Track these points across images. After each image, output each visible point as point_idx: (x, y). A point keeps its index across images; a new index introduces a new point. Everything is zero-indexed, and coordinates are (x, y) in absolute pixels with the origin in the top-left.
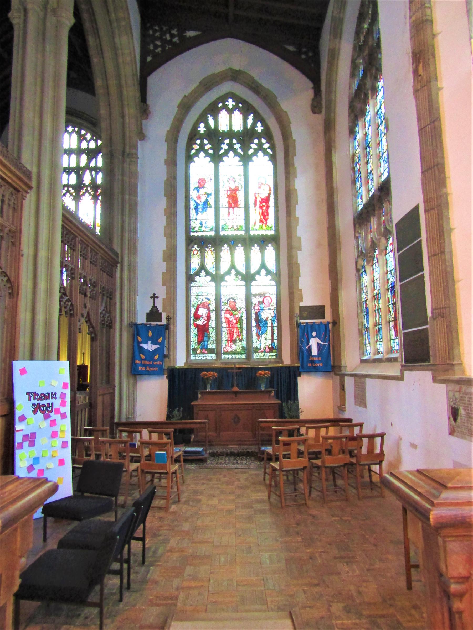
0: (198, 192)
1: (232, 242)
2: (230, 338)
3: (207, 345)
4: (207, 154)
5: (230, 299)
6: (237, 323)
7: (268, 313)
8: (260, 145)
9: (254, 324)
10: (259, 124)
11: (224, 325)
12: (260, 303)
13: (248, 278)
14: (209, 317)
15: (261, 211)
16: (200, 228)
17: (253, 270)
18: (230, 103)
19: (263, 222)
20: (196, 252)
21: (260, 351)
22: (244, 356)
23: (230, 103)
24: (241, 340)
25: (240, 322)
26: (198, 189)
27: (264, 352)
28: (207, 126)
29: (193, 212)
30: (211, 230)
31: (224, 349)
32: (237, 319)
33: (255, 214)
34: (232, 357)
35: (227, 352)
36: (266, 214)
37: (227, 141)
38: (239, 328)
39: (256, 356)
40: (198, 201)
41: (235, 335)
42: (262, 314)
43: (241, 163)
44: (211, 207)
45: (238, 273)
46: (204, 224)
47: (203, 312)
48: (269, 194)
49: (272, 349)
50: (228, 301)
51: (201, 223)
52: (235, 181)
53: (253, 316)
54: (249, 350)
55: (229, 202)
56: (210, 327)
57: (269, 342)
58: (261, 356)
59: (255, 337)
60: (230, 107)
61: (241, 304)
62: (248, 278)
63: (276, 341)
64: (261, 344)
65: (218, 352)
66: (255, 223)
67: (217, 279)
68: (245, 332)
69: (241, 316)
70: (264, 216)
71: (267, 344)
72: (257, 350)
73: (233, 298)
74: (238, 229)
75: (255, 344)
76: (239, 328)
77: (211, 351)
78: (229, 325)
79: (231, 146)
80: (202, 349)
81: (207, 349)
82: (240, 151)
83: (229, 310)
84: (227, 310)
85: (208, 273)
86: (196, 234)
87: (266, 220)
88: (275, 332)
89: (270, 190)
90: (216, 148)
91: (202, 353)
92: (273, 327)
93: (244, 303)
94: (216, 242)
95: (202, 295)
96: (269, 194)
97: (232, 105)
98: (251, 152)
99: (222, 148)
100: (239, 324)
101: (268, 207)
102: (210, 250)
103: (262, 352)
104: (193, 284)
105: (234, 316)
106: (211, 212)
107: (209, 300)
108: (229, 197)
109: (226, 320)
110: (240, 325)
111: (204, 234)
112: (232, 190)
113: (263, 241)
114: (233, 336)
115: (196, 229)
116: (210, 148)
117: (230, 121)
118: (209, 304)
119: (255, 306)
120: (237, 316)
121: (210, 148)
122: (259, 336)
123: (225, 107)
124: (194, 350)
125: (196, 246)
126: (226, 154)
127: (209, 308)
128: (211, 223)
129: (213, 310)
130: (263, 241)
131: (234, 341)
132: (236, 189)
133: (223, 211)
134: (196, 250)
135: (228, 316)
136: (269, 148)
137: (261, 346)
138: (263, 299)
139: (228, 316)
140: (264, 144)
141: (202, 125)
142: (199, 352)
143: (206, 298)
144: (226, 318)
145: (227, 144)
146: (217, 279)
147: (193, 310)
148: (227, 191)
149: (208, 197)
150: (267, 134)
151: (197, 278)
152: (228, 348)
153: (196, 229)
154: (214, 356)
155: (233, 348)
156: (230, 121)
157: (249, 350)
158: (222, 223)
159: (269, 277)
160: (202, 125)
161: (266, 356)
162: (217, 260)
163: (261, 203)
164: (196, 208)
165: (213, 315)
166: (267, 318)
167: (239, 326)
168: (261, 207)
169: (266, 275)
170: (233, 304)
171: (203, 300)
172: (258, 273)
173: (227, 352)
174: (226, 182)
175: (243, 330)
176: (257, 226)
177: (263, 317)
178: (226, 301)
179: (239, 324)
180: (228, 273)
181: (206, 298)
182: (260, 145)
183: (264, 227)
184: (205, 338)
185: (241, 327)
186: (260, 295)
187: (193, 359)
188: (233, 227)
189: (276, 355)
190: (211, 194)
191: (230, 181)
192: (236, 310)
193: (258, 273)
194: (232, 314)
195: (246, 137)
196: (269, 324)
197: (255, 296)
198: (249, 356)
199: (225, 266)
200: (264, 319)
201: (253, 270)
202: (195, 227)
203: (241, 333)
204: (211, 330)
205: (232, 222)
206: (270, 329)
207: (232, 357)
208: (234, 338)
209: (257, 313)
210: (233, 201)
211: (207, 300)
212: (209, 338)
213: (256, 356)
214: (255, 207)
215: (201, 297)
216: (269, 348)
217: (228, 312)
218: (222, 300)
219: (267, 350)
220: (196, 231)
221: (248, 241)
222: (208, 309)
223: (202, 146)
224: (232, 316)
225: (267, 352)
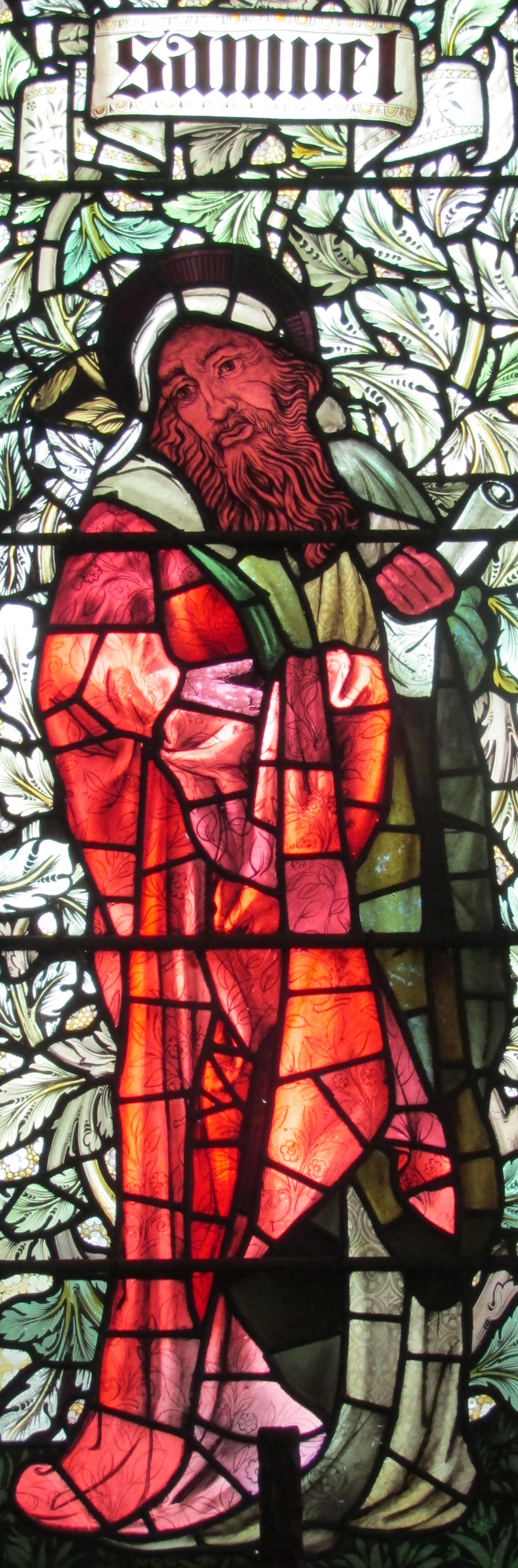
2: (183, 1205)
5: (164, 272)
6: (347, 852)
25: (431, 826)
38: (401, 973)
50: (124, 310)
76: (401, 973)
83: (160, 539)
100: (388, 859)
105: (284, 661)
109: (90, 781)
110: (431, 877)
114: (254, 1159)
120: (349, 679)
131: (291, 1298)
135: (133, 671)
139: (133, 671)
170: (252, 391)
178: (70, 325)
179: (388, 859)
192: (332, 525)
194: (235, 632)
208: (286, 1205)
217: (116, 583)
224: (216, 686)
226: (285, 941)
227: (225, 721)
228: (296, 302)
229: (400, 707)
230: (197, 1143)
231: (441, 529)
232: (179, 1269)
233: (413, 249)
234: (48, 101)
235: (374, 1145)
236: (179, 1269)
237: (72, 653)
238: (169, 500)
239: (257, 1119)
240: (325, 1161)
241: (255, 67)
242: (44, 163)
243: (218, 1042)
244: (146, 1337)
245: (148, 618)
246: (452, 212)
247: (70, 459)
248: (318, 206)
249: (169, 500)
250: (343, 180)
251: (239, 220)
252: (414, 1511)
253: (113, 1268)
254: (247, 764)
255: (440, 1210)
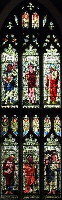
0: (7, 75)
1: (31, 113)
3: (12, 188)
4: (14, 46)
5: (29, 155)
6: (33, 173)
7: (55, 166)
8: (52, 40)
9: (45, 174)
10: (51, 24)
11: (24, 174)
12: (50, 158)
13: (41, 140)
14: (14, 168)
15: (51, 90)
16: (8, 102)
17: (45, 135)
18: (31, 6)
19: (53, 99)
20: (5, 120)
21: (49, 193)
22: (38, 197)
23: (31, 6)
24: (36, 185)
26: (7, 73)
27: (52, 194)
28: (14, 23)
29: (3, 90)
30: (16, 104)
31: (24, 191)
32: (33, 170)
33: (47, 94)
34: (30, 197)
35: (26, 194)
36: (55, 93)
37: (28, 36)
39: (45, 197)
40: (7, 82)
41: (32, 182)
42: (51, 166)
43: (37, 54)
44: (16, 86)
45: (34, 136)
46: (11, 98)
47: (10, 164)
48: (58, 78)
49: (57, 192)
51: (9, 98)
52: (33, 67)
53: (45, 167)
54: (41, 192)
55: (28, 83)
56: (15, 175)
57: (56, 187)
58: (50, 197)
59: (45, 183)
60: (31, 9)
61: (36, 159)
62: (41, 140)
63: (60, 186)
64: (49, 188)
65: (20, 193)
66: (47, 99)
67: (20, 140)
68: (38, 179)
69: (37, 168)
70: (54, 94)
71: (54, 188)
72: (47, 192)
73: (30, 155)
74: (34, 104)
75: (46, 188)
76: (35, 177)
77: (15, 193)
78: (28, 174)
79: (31, 39)
80: (9, 192)
81: (13, 192)
82: (37, 44)
84: (26, 163)
85: (14, 136)
86: (5, 107)
87: (55, 97)
88: (60, 180)
89: (58, 74)
90: (20, 41)
91: (9, 194)
92: (58, 176)
93: (39, 159)
94: (20, 113)
95: (9, 152)
96: (58, 78)
97: (32, 8)
98: (45, 44)
99: (24, 42)
100: (34, 173)
101: (57, 87)
102: (15, 119)
103: (50, 194)
104: (3, 144)
105: (31, 167)
106: (16, 90)
107: (14, 155)
108: (29, 79)
111: (11, 107)
112: (30, 74)
113: (52, 113)
115: (5, 103)
116: (16, 42)
117: (31, 21)
118: (14, 159)
119: (46, 161)
121: (16, 42)
122: (48, 182)
123: (27, 9)
124: (4, 192)
125: (5, 116)
126: (27, 46)
127: (14, 162)
128: (16, 99)
129: (17, 163)
130: (52, 113)
131: (31, 186)
132: (34, 73)
133: (25, 89)
134: (5, 118)
135: (27, 167)
136: (58, 42)
137: (49, 190)
138: (52, 156)
139: (27, 167)
140: (54, 39)
141: (10, 23)
142: (7, 193)
143: (12, 154)
144: (26, 169)
145: (28, 39)
146: (20, 140)
147: (3, 162)
148: (28, 74)
149: (14, 79)
150: (56, 31)
151: (6, 140)
152: (27, 191)
153: (5, 103)
154: (17, 197)
155: (31, 191)
156: (31, 21)
157: (41, 192)
158: (24, 98)
159: (56, 140)
160: (10, 23)
161: (53, 197)
162: (20, 126)
163: (51, 84)
164: (5, 87)
165: (17, 167)
166: (55, 170)
167: (35, 175)
168: (51, 88)
169: (54, 138)
171: (10, 155)
172: (49, 136)
173: (26, 194)
174: (27, 67)
175: (37, 178)
176: (49, 102)
177: (52, 168)
178: (26, 157)
179: (34, 173)
180: (28, 136)
181: (12, 154)
182: (52, 40)
183: (53, 102)
184: (11, 184)
185: (36, 176)
186: (50, 152)
187: (3, 198)
188: (31, 101)
189: (60, 197)
190: (16, 76)
191: (30, 67)
192: (33, 163)
193: (49, 136)
195: (42, 32)
196: (56, 174)
197: (46, 153)
198: (41, 196)
199: (25, 131)
200: (52, 170)
201: (45, 135)
202: (5, 102)
203: (36, 180)
204: (15, 178)
205: (31, 96)
206: (56, 177)
207: (30, 197)
208: (31, 183)
209: (48, 165)
210: (32, 83)
211: (13, 156)
212: (14, 183)
213: (45, 197)
214: (47, 87)
215: (8, 153)
216: (55, 191)
217: (27, 165)
218: (24, 156)
219: (54, 192)
220: (6, 105)
221: (41, 113)
222: (14, 162)
223: (10, 39)
224: (30, 168)
225: (54, 194)
226: (31, 176)
227: (30, 169)
228: (32, 156)
229: (35, 169)
230: (29, 181)
231: (36, 163)
232: (28, 185)
233: (35, 154)
234: (25, 149)
235: (34, 182)
236: (28, 185)
237: (26, 167)
238: (28, 162)
239: (31, 181)
240: (32, 182)
241: (31, 148)
242: (25, 152)
243: (29, 179)
244: (27, 187)
245: (28, 166)
246: (37, 153)
247: (26, 161)
248: (33, 153)
249: (28, 162)
250: (33, 152)
251: (31, 153)
252: (35, 192)
253: (26, 185)
254: (30, 170)
255: (36, 184)
